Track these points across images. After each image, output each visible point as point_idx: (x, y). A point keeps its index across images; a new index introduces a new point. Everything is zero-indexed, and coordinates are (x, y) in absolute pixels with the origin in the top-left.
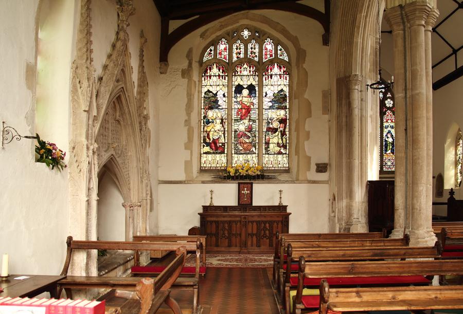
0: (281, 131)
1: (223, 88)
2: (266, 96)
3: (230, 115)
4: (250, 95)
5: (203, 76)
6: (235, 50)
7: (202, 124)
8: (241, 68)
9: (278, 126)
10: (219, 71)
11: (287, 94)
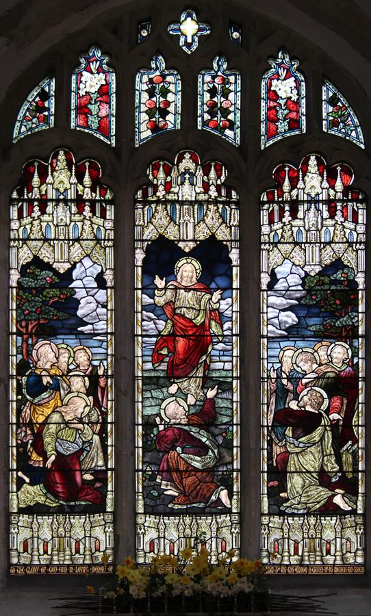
0: (334, 425)
1: (98, 254)
2: (271, 286)
3: (124, 358)
4: (206, 282)
5: (12, 202)
6: (145, 96)
7: (13, 396)
8: (168, 173)
9: (320, 404)
10: (80, 180)
11: (360, 279)
